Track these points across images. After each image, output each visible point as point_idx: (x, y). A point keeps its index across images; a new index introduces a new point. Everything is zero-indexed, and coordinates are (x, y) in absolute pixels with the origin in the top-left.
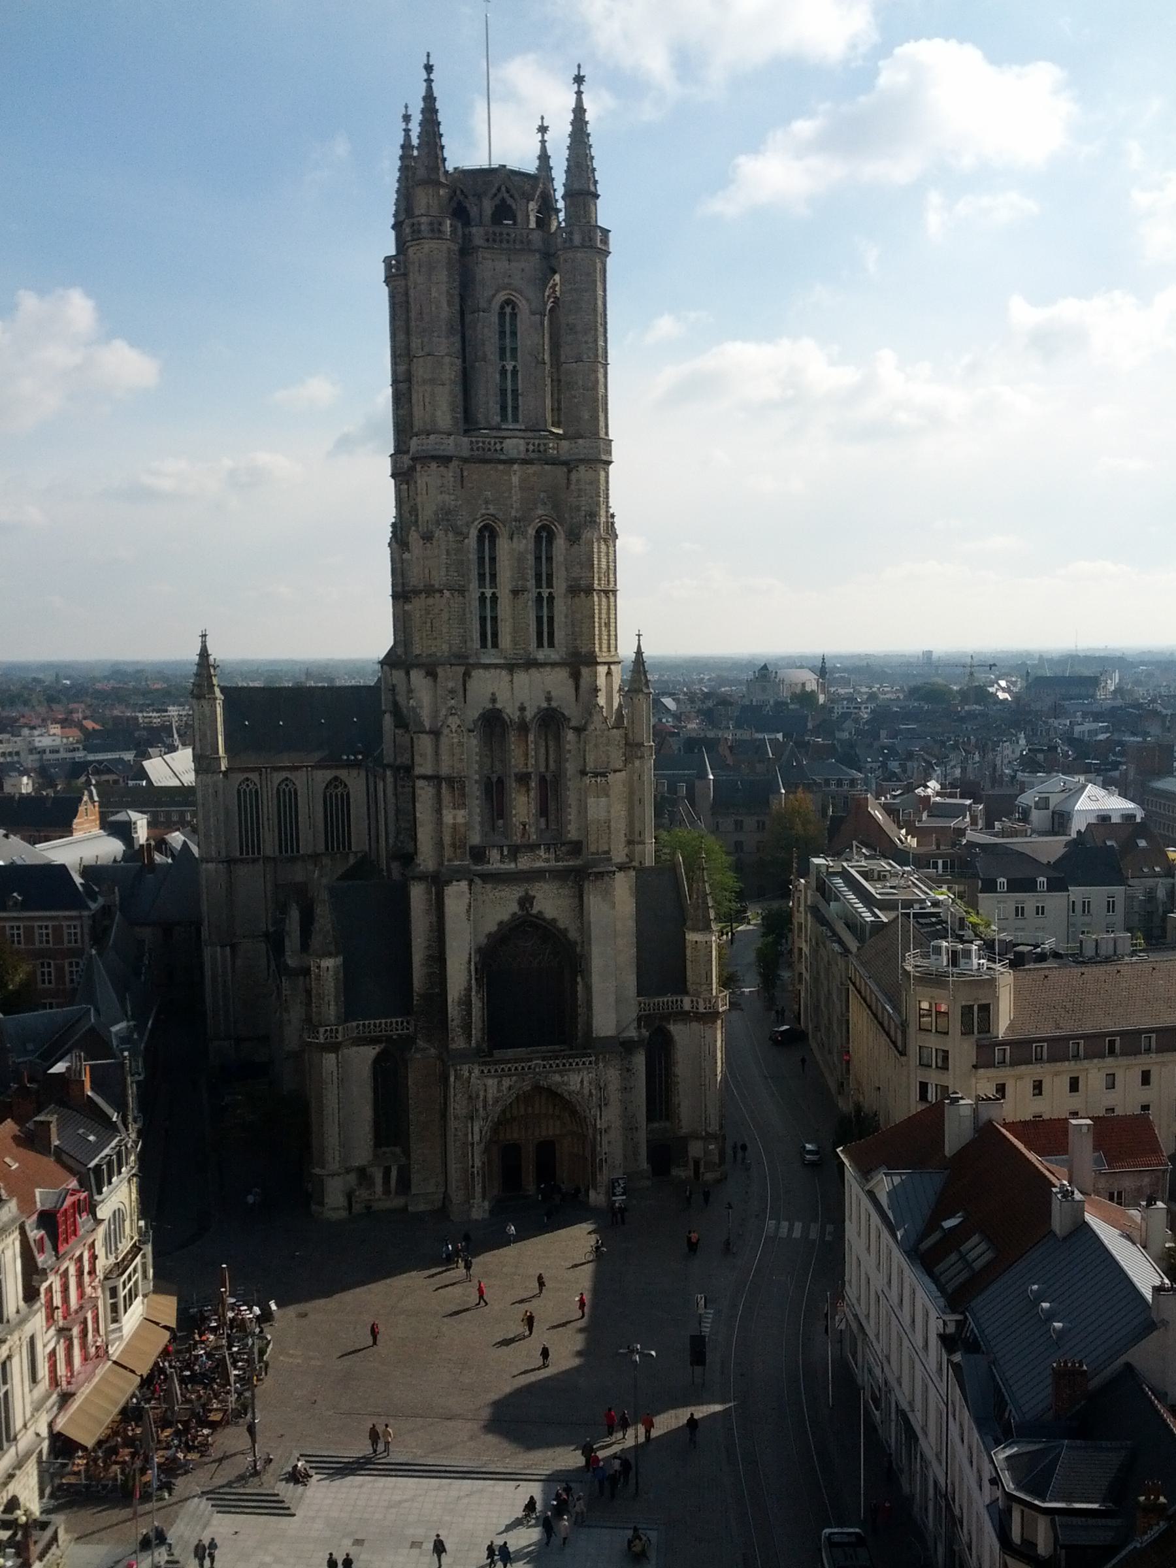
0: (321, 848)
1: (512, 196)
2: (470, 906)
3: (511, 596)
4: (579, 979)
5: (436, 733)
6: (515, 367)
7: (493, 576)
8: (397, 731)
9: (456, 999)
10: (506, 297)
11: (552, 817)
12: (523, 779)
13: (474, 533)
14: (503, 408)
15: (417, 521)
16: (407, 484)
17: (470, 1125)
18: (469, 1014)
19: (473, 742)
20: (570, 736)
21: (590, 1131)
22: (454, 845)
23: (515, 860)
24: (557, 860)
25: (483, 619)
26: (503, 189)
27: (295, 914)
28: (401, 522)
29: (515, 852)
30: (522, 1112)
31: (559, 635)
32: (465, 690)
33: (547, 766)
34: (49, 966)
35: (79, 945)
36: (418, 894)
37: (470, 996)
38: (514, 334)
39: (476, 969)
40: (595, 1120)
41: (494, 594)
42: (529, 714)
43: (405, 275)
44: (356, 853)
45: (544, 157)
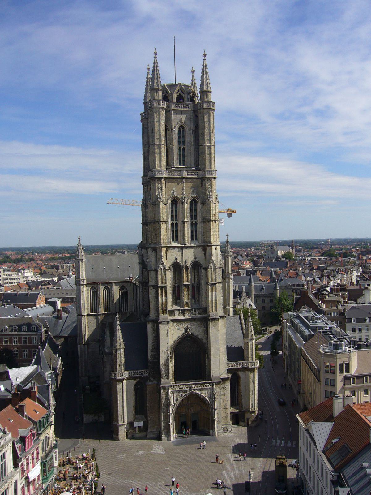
0: (118, 310)
1: (183, 93)
2: (168, 331)
3: (182, 223)
4: (206, 356)
5: (156, 271)
6: (183, 147)
7: (176, 216)
8: (143, 270)
9: (163, 363)
10: (181, 125)
11: (196, 299)
12: (186, 286)
13: (170, 202)
14: (180, 161)
15: (150, 199)
16: (148, 186)
17: (168, 407)
18: (168, 368)
19: (169, 274)
20: (203, 271)
21: (211, 410)
22: (162, 309)
23: (184, 315)
24: (198, 314)
25: (173, 231)
26: (180, 90)
27: (108, 333)
28: (145, 198)
29: (183, 312)
30: (187, 402)
31: (199, 236)
32: (166, 255)
33: (195, 281)
34: (26, 351)
35: (37, 344)
36: (150, 326)
37: (168, 362)
38: (183, 137)
39: (170, 353)
40: (212, 406)
41: (176, 222)
42: (189, 264)
43: (148, 119)
44: (129, 312)
45: (193, 80)
